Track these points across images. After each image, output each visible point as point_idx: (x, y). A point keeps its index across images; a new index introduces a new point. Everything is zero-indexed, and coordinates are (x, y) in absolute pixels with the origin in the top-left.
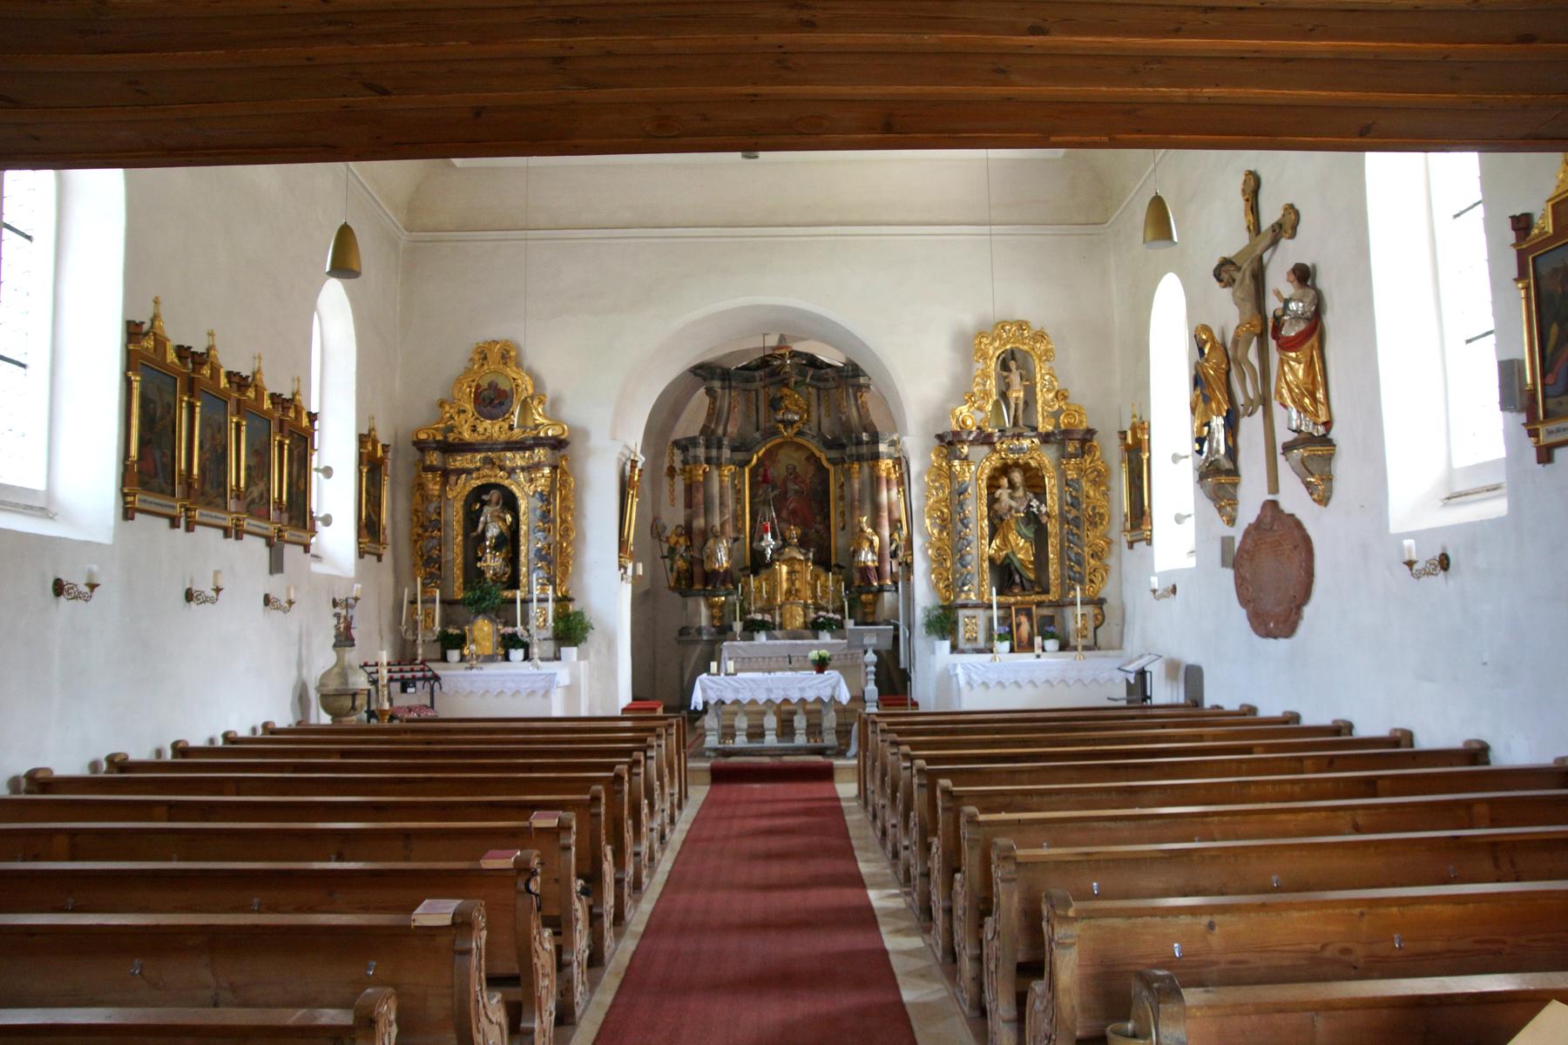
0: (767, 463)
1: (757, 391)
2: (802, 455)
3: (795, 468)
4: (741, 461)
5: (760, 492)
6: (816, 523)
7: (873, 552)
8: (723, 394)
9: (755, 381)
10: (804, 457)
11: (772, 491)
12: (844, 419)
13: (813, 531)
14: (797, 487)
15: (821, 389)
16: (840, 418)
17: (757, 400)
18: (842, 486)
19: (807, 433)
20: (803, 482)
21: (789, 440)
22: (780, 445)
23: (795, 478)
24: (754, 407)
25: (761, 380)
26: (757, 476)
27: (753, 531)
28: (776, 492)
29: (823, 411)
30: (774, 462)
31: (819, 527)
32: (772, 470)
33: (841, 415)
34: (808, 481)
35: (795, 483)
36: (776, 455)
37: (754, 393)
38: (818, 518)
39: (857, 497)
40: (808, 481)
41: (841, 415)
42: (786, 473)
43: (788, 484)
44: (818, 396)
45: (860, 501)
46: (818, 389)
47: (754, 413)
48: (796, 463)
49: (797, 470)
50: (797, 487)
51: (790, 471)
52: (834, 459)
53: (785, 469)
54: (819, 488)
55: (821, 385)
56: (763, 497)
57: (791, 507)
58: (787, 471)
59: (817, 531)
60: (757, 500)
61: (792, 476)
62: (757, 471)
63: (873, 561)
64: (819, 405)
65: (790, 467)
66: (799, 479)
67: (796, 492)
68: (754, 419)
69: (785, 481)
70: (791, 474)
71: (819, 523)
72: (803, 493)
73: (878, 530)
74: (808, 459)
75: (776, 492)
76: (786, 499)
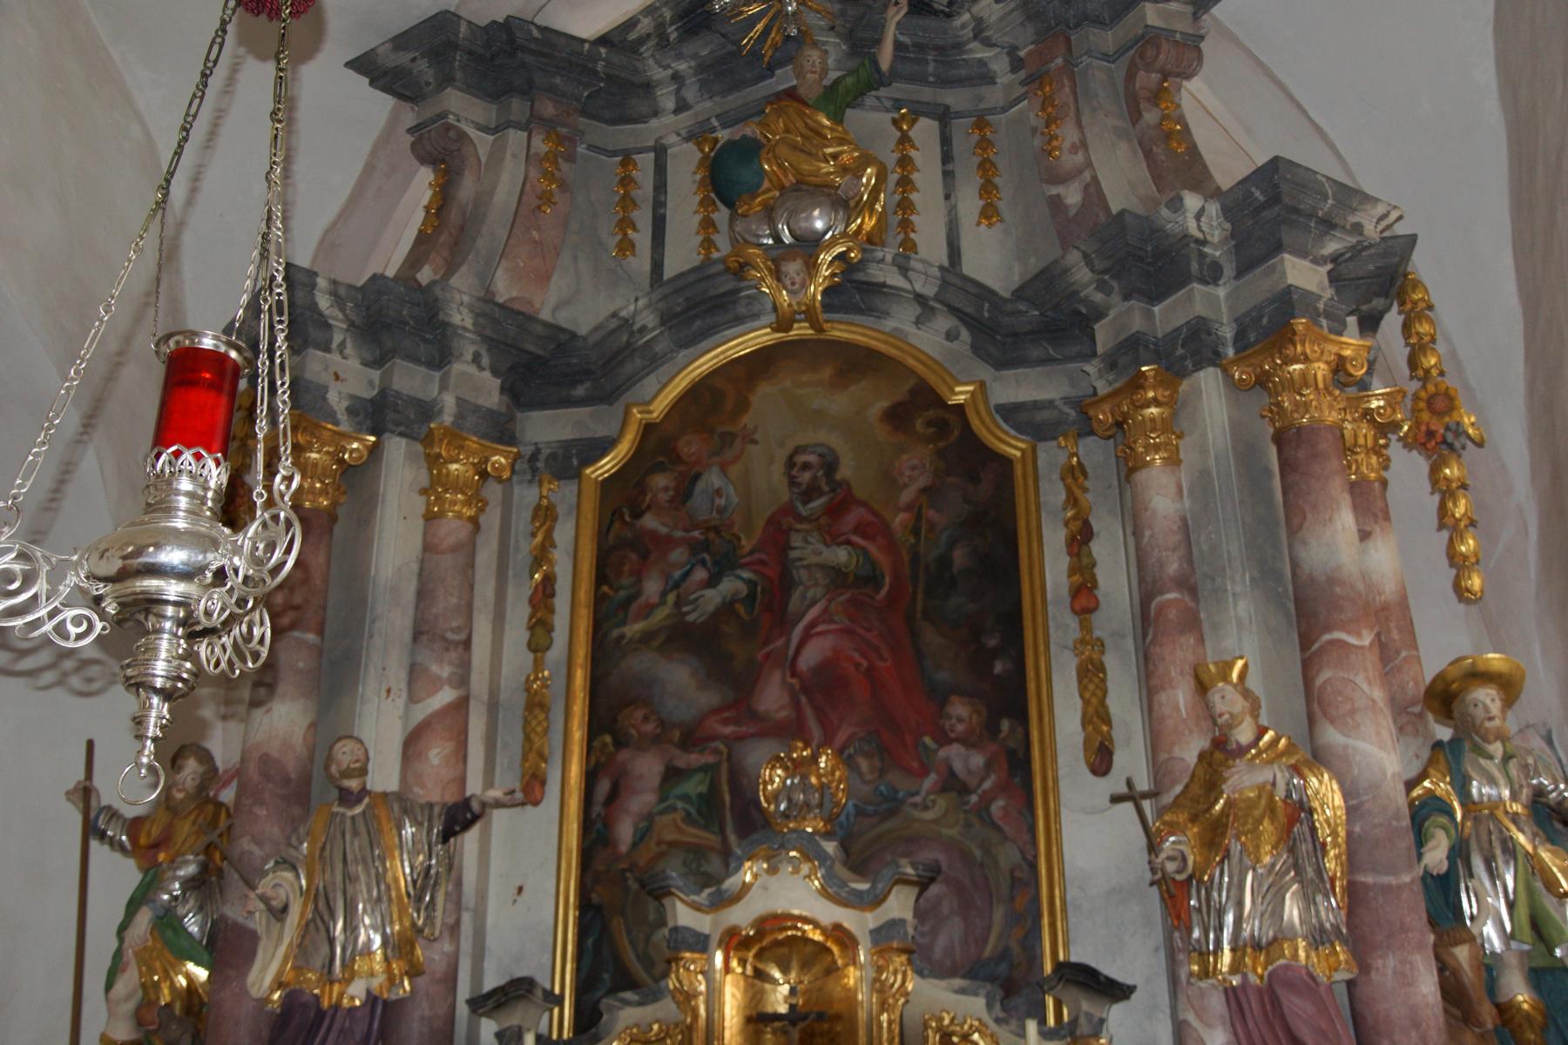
0: (690, 446)
1: (660, 152)
2: (876, 401)
3: (830, 464)
4: (567, 445)
5: (652, 587)
6: (944, 739)
7: (1314, 886)
8: (497, 153)
9: (656, 113)
10: (882, 404)
11: (712, 582)
12: (1072, 196)
13: (930, 781)
14: (841, 555)
15: (959, 115)
16: (1056, 203)
17: (660, 186)
18: (1080, 538)
19: (879, 288)
20: (875, 528)
21: (801, 330)
22: (760, 363)
23: (835, 511)
24: (643, 217)
25: (682, 107)
26: (637, 514)
27: (604, 787)
28: (730, 586)
29: (969, 203)
30: (727, 439)
31: (966, 760)
32: (713, 478)
33: (1054, 190)
34: (899, 520)
35: (834, 538)
36: (743, 406)
37: (646, 161)
38: (960, 711)
39: (1173, 567)
40: (899, 520)
41: (1054, 190)
42: (785, 495)
43: (796, 540)
44: (946, 140)
45: (1187, 584)
46: (944, 116)
47: (642, 238)
48: (835, 441)
49: (845, 471)
50: (841, 555)
51: (806, 477)
52: (1037, 406)
53: (778, 468)
54: (959, 557)
55: (954, 98)
56: (660, 615)
57: (812, 655)
58: (792, 482)
59: (953, 784)
60: (634, 629)
61: (817, 504)
62: (642, 488)
63: (1319, 937)
64: (948, 175)
65: (812, 458)
66: (854, 516)
67: (838, 578)
68: (641, 263)
69: (778, 534)
70: (809, 493)
71: (966, 741)
72: (873, 580)
73: (1331, 736)
74: (897, 416)
75: (730, 586)
76: (783, 623)
